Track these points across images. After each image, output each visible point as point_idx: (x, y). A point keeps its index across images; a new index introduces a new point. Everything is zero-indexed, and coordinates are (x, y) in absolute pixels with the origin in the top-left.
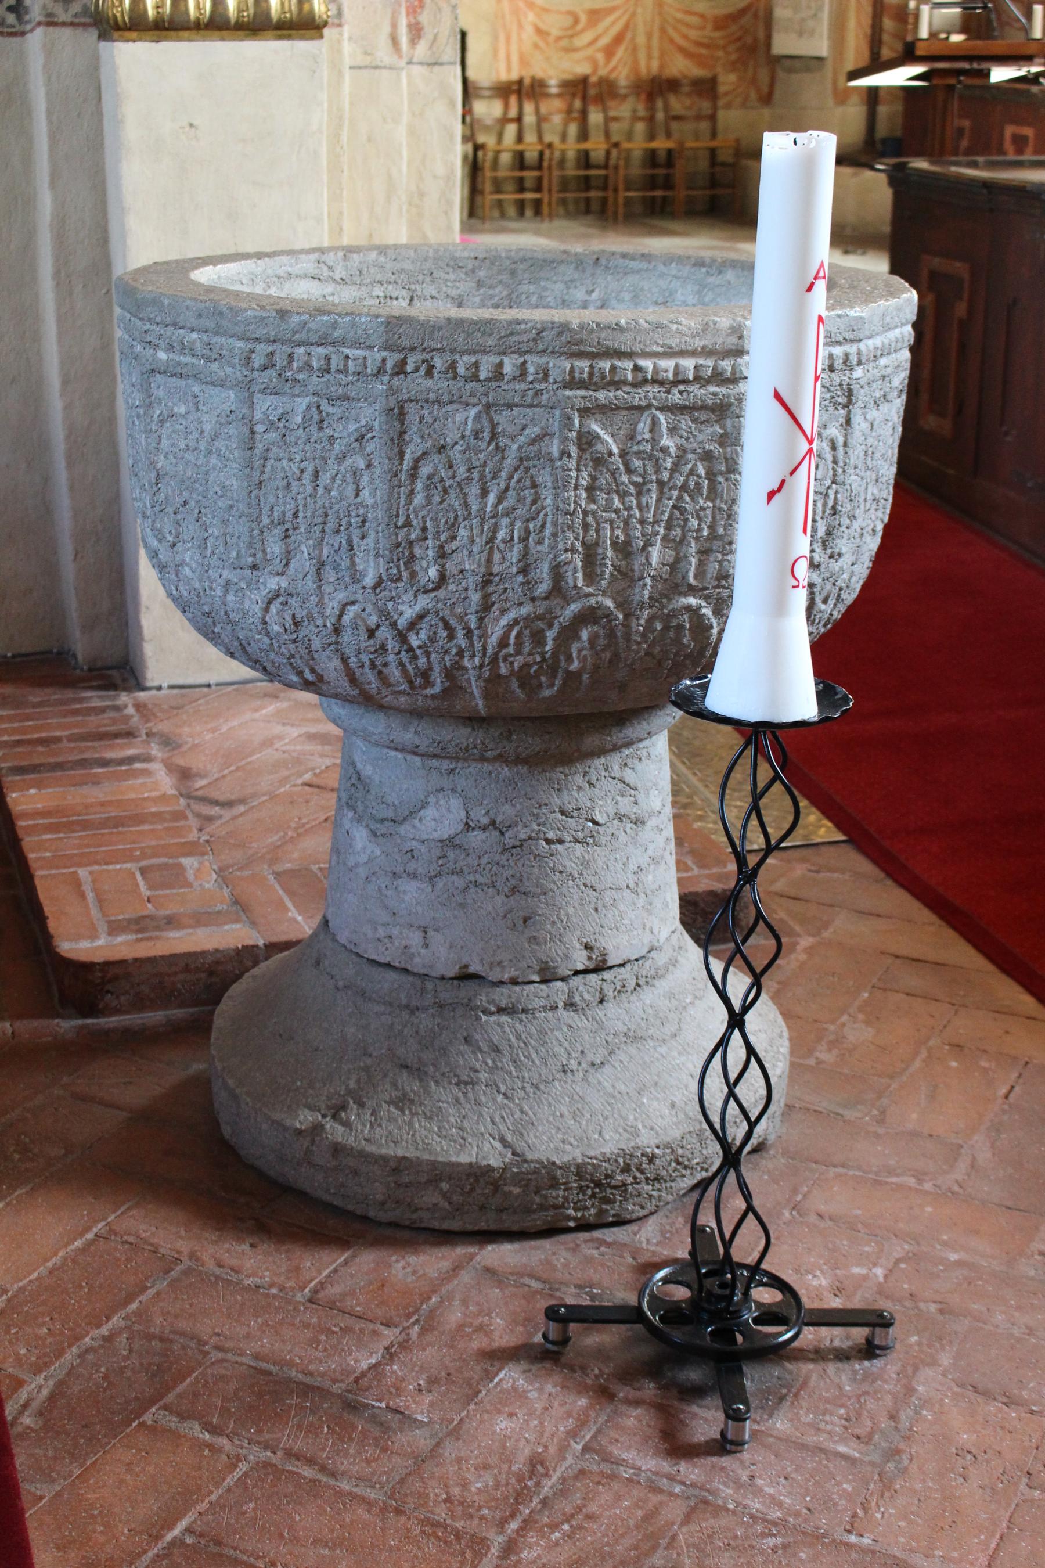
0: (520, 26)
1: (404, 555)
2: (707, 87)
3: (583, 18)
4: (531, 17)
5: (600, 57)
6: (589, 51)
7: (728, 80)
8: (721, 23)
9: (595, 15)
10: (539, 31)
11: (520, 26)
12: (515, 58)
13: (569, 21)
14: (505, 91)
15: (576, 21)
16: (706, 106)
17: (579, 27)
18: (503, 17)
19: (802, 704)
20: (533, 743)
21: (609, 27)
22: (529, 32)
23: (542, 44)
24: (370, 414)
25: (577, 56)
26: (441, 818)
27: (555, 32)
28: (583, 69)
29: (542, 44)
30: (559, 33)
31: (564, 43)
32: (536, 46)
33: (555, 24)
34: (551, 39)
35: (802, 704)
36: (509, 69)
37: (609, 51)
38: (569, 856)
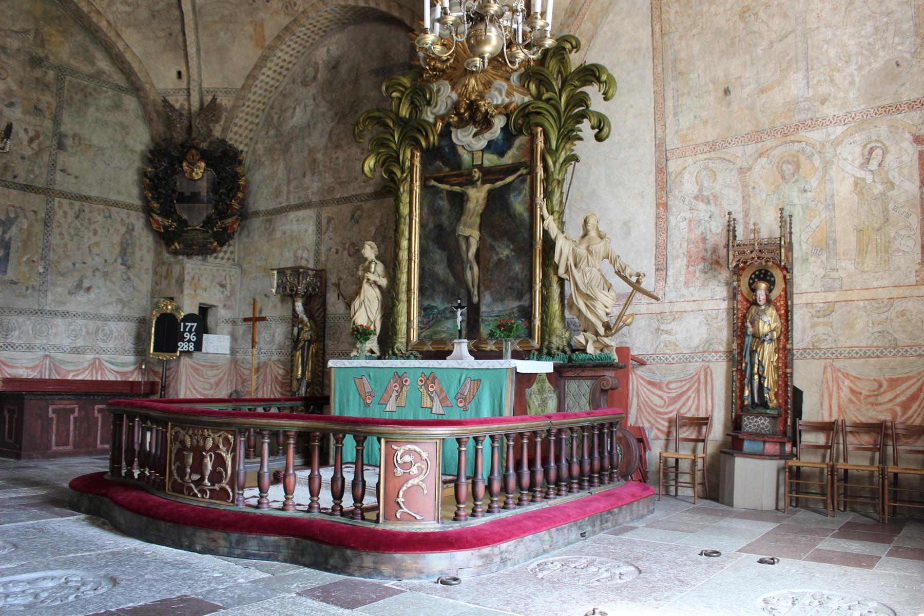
0: (839, 388)
3: (885, 384)
4: (847, 382)
5: (898, 410)
6: (890, 405)
9: (894, 383)
10: (852, 391)
11: (839, 388)
12: (835, 408)
13: (876, 385)
14: (827, 428)
15: (880, 386)
17: (882, 390)
18: (827, 382)
21: (906, 391)
22: (845, 393)
23: (854, 399)
25: (879, 408)
27: (865, 393)
28: (885, 416)
29: (854, 399)
30: (868, 393)
31: (871, 400)
32: (851, 401)
33: (865, 388)
34: (862, 397)
36: (831, 415)
37: (905, 406)
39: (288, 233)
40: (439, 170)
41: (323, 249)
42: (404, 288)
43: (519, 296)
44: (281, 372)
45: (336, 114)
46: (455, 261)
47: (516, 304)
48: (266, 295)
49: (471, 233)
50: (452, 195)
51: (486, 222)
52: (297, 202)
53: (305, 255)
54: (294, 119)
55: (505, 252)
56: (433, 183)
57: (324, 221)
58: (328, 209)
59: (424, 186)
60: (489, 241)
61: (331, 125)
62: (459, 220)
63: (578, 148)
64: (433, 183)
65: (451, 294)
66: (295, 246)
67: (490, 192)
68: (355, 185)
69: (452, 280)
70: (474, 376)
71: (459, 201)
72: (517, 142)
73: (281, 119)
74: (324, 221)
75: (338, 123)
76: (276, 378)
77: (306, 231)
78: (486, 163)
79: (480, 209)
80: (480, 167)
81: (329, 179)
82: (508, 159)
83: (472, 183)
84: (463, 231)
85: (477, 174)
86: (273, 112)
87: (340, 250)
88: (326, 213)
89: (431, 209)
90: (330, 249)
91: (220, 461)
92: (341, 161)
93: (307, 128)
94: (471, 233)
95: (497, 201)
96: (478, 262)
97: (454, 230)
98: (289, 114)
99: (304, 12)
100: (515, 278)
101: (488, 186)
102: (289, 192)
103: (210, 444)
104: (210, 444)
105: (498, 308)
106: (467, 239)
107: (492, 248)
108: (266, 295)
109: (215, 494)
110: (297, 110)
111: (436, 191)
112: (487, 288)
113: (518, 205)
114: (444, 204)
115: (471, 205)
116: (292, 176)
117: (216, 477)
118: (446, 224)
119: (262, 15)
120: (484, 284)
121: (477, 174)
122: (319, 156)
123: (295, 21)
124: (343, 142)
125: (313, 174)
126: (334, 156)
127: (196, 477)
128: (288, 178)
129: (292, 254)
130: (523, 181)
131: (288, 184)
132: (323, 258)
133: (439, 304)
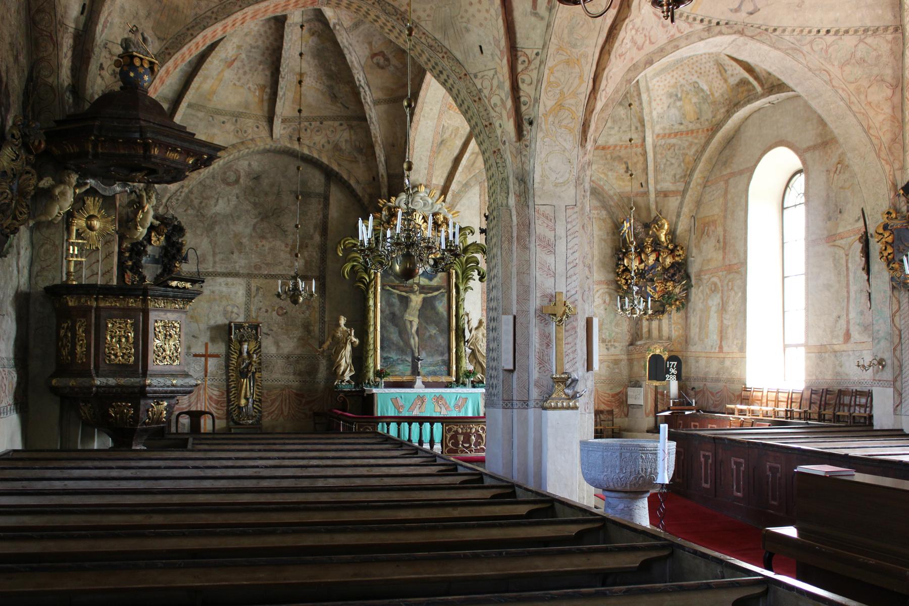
1: (621, 470)
2: (611, 412)
7: (616, 411)
8: (613, 396)
16: (610, 417)
19: (667, 482)
20: (632, 496)
24: (618, 454)
26: (621, 506)
35: (667, 482)
38: (637, 511)
39: (217, 292)
40: (392, 282)
41: (253, 308)
42: (372, 347)
43: (442, 354)
44: (216, 393)
45: (260, 214)
46: (403, 333)
47: (440, 358)
48: (193, 336)
49: (413, 319)
50: (401, 298)
51: (422, 314)
52: (223, 270)
53: (235, 310)
54: (217, 208)
55: (433, 331)
56: (388, 288)
57: (254, 289)
58: (256, 280)
59: (382, 289)
60: (424, 324)
61: (255, 220)
62: (405, 311)
63: (471, 283)
64: (388, 288)
65: (402, 351)
66: (224, 303)
67: (424, 299)
68: (281, 267)
69: (402, 343)
70: (463, 396)
71: (405, 301)
72: (440, 274)
73: (203, 204)
74: (254, 289)
75: (262, 220)
76: (210, 398)
77: (236, 293)
78: (422, 283)
79: (419, 307)
80: (418, 284)
81: (255, 259)
82: (435, 282)
83: (413, 292)
84: (408, 317)
85: (416, 288)
86: (193, 197)
87: (270, 310)
88: (254, 283)
89: (388, 303)
90: (260, 309)
91: (480, 436)
92: (267, 248)
93: (232, 217)
94: (413, 319)
95: (428, 304)
96: (418, 335)
97: (403, 317)
98: (213, 202)
99: (252, 140)
100: (440, 345)
101: (423, 295)
102: (215, 262)
103: (474, 430)
104: (474, 430)
105: (430, 360)
106: (411, 322)
107: (426, 328)
108: (193, 336)
109: (477, 451)
110: (220, 201)
111: (391, 293)
112: (423, 349)
113: (441, 307)
114: (396, 301)
115: (413, 304)
116: (217, 251)
117: (477, 444)
118: (398, 312)
119: (215, 131)
120: (421, 346)
121: (416, 288)
122: (245, 241)
123: (243, 143)
124: (269, 235)
125: (240, 253)
126: (260, 244)
127: (467, 445)
128: (214, 251)
129: (221, 308)
130: (443, 296)
131: (214, 255)
132: (254, 315)
133: (394, 356)
